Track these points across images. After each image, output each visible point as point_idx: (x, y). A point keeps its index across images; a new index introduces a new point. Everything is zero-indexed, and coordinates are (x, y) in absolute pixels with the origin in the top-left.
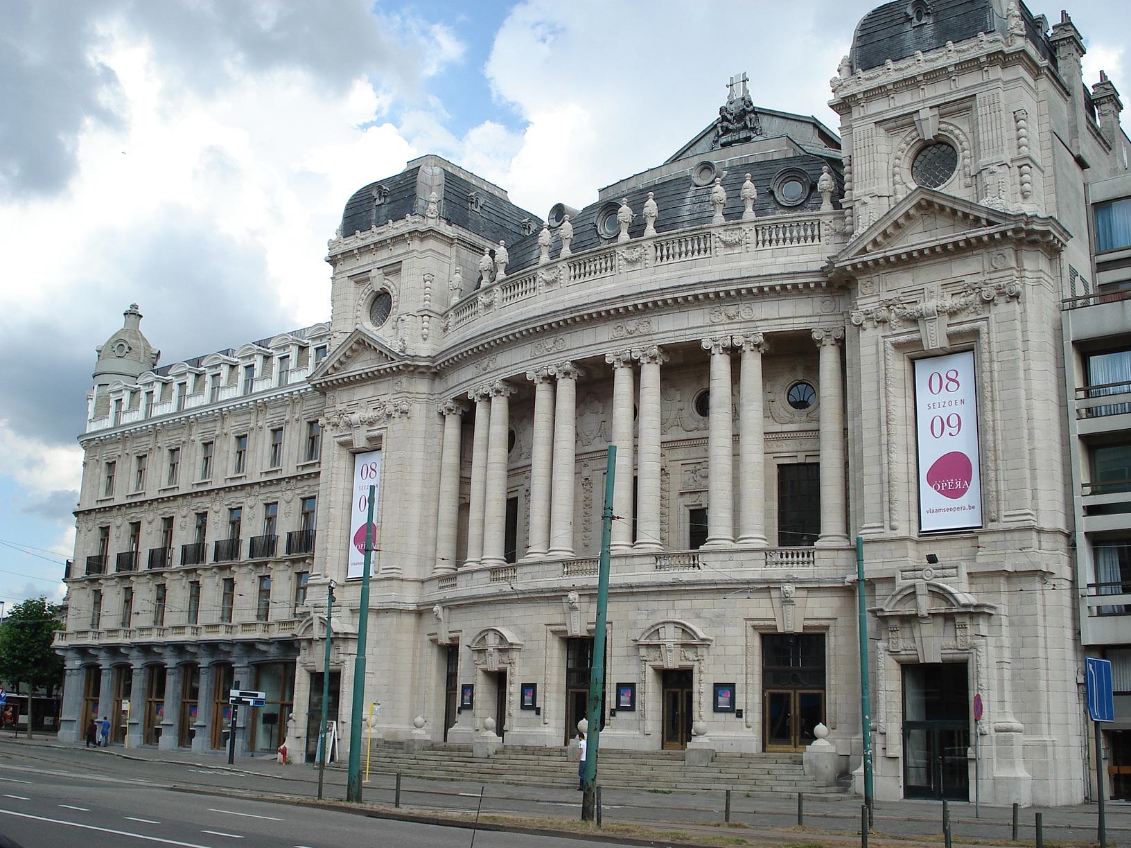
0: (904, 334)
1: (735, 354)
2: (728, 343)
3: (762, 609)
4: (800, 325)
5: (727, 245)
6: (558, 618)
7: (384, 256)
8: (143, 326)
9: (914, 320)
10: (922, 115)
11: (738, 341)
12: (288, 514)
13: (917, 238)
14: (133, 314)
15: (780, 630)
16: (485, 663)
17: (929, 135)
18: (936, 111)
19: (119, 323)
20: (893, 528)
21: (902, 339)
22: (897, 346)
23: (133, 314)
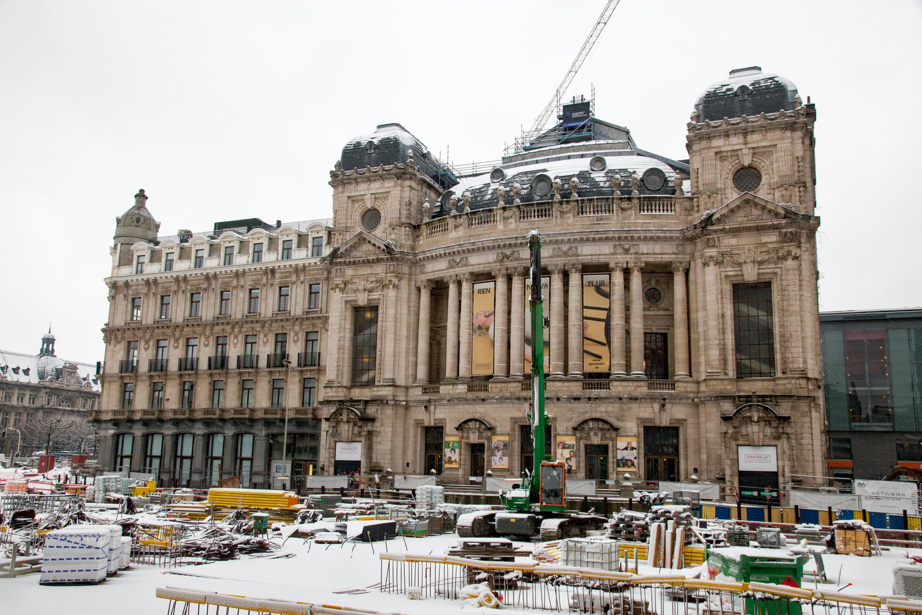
0: (731, 271)
1: (627, 272)
2: (625, 266)
3: (648, 411)
4: (666, 258)
5: (623, 209)
6: (519, 414)
7: (376, 187)
8: (148, 204)
9: (740, 265)
10: (745, 151)
11: (631, 265)
12: (295, 342)
13: (739, 220)
14: (141, 196)
15: (657, 424)
16: (468, 438)
17: (746, 164)
18: (752, 151)
19: (132, 202)
20: (726, 374)
21: (731, 273)
22: (726, 276)
23: (141, 196)
